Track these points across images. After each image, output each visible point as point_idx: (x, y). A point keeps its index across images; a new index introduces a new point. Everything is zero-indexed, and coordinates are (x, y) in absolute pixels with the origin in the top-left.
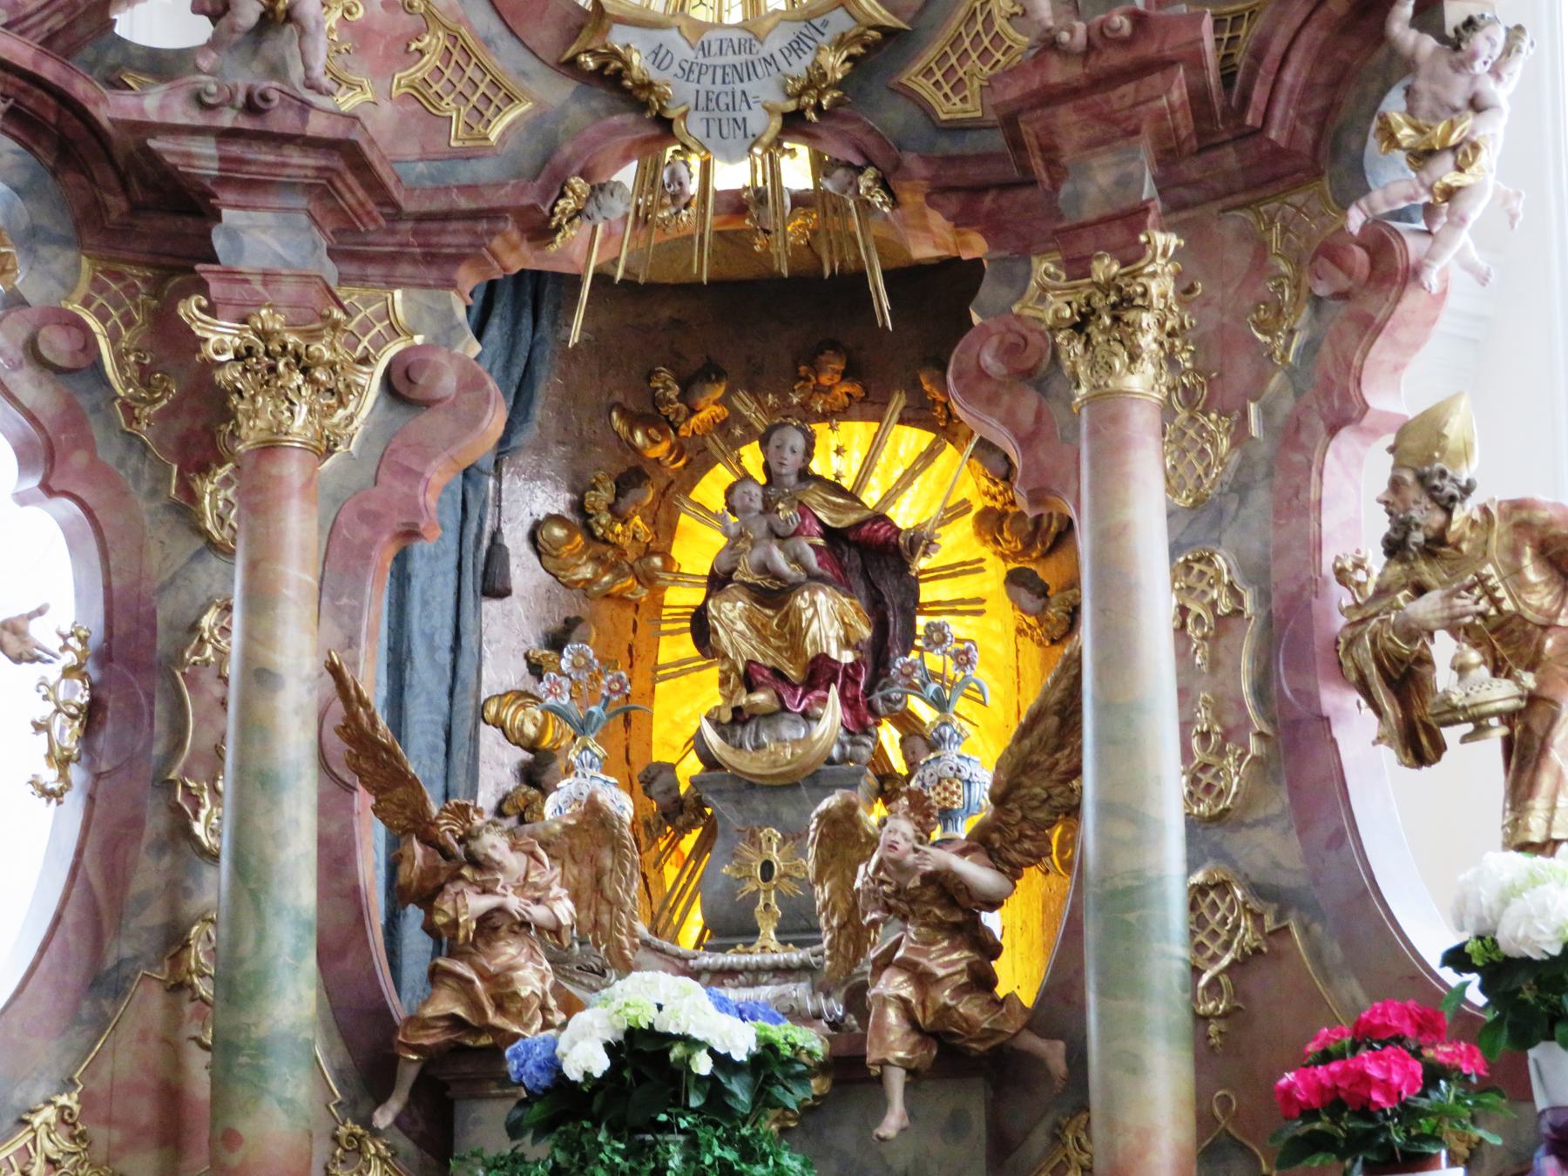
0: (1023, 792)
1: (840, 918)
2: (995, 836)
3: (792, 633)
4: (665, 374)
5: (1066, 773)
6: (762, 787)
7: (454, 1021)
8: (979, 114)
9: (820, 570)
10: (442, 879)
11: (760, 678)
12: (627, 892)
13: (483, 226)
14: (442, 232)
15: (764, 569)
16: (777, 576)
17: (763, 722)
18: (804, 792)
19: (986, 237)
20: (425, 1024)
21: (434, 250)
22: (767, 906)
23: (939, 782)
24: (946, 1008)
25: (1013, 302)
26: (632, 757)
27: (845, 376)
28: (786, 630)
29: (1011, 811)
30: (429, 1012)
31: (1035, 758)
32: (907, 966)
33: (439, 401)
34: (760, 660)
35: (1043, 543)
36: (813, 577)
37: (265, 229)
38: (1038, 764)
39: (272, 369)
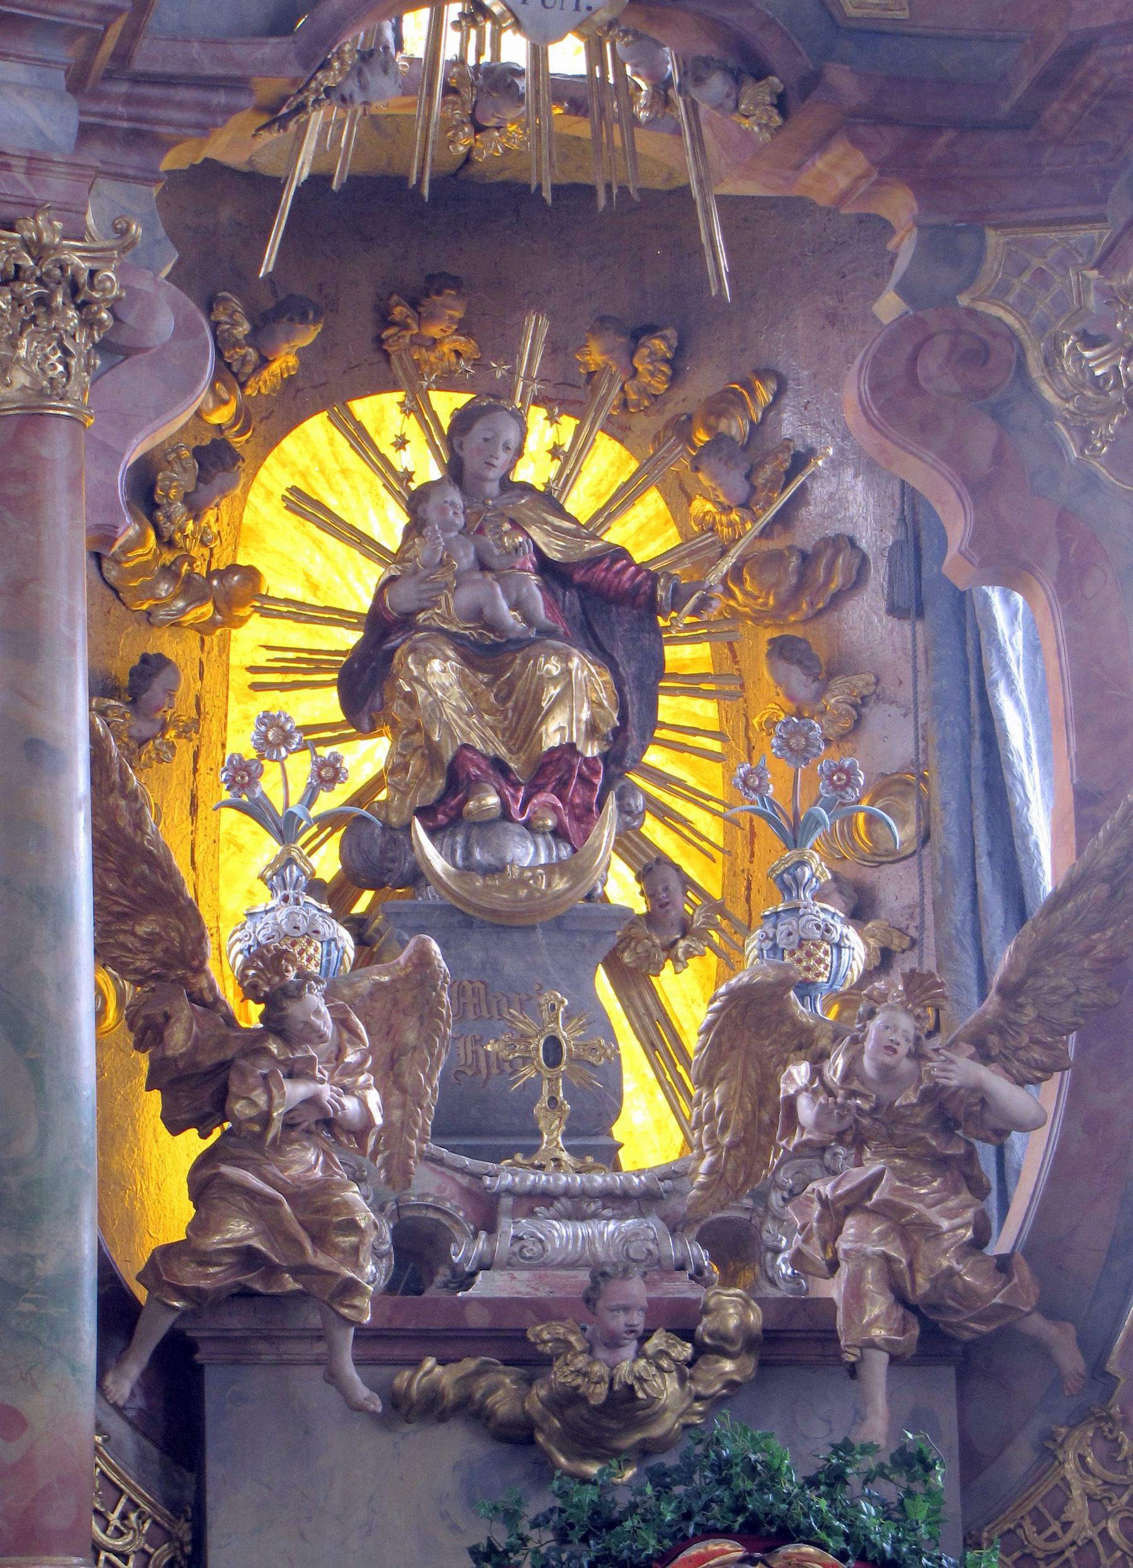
0: (1041, 982)
1: (735, 1134)
2: (994, 1040)
3: (519, 710)
4: (236, 303)
5: (1104, 960)
6: (483, 925)
7: (248, 1257)
8: (905, 15)
9: (549, 622)
10: (229, 1054)
11: (473, 770)
12: (429, 1079)
13: (220, 98)
14: (164, 102)
15: (478, 615)
16: (492, 625)
17: (475, 832)
18: (539, 936)
19: (918, 197)
20: (205, 1259)
21: (145, 127)
22: (553, 1101)
23: (801, 946)
24: (951, 1273)
25: (961, 290)
26: (198, 858)
27: (464, 328)
28: (510, 704)
29: (1021, 1006)
30: (215, 1241)
31: (1064, 938)
32: (889, 1211)
33: (146, 350)
34: (479, 746)
35: (812, 604)
36: (550, 633)
37: (20, 89)
38: (1068, 944)
39: (42, 301)
